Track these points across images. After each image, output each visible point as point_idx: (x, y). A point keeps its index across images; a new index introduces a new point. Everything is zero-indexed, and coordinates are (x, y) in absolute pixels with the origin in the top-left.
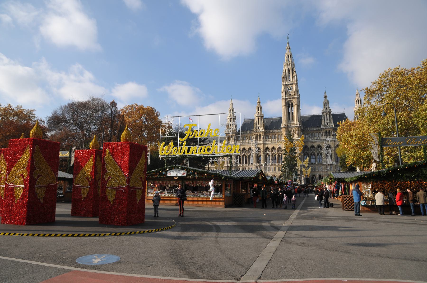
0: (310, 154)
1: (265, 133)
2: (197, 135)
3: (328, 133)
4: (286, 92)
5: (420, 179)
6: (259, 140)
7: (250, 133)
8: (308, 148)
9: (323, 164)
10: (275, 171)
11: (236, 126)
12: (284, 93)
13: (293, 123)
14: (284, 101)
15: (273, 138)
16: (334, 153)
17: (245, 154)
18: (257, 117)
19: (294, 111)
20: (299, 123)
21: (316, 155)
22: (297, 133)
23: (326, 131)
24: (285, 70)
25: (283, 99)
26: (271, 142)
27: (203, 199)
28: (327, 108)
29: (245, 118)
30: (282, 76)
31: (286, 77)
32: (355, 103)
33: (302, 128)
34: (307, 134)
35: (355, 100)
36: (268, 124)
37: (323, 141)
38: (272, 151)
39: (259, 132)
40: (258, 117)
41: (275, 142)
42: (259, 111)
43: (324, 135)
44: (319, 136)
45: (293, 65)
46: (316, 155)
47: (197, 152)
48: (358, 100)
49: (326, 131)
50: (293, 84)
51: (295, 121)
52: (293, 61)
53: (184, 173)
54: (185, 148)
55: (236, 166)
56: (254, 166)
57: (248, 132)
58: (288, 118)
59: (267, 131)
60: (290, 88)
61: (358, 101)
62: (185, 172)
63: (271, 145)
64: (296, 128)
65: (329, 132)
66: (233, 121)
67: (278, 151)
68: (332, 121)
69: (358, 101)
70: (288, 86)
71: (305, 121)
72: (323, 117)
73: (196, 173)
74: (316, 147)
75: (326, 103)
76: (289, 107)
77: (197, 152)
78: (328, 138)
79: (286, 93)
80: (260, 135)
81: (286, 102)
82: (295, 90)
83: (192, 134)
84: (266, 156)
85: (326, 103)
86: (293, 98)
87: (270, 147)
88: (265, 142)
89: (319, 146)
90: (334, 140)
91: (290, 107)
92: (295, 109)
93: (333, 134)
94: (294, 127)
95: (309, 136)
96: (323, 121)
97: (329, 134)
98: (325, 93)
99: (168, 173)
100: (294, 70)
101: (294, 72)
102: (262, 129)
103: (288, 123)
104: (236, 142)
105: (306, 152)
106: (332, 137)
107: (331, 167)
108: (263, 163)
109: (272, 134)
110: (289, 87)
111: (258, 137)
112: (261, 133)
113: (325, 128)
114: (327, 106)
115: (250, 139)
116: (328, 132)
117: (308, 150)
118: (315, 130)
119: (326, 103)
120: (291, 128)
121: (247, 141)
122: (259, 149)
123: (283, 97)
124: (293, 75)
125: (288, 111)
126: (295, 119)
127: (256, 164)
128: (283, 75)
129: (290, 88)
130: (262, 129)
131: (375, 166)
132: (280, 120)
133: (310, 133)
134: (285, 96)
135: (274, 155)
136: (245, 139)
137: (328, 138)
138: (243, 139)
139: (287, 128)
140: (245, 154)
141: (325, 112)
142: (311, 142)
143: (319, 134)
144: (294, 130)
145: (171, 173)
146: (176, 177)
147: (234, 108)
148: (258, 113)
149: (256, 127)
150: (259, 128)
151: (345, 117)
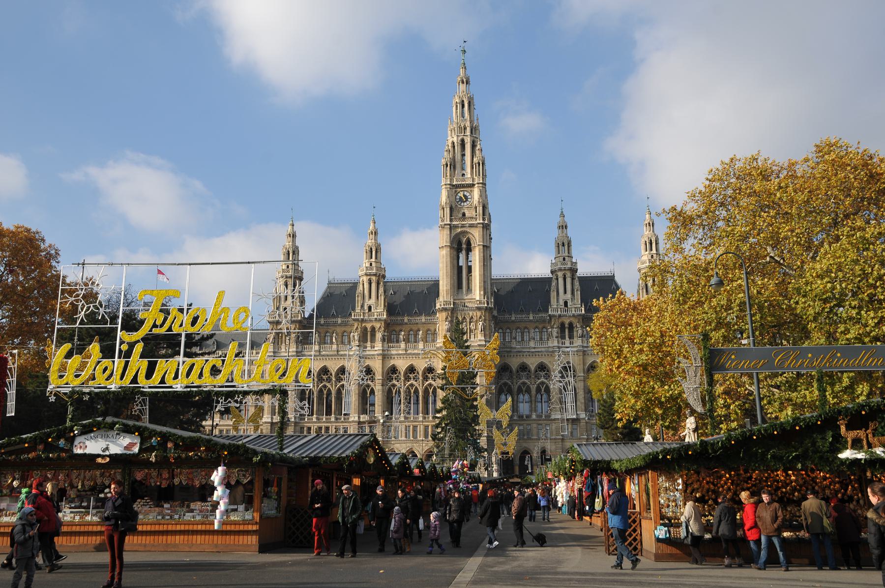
1: (388, 325)
2: (181, 325)
3: (567, 330)
4: (454, 206)
5: (811, 466)
6: (369, 343)
7: (345, 324)
8: (511, 372)
9: (552, 420)
10: (413, 437)
11: (302, 302)
12: (447, 211)
13: (469, 297)
14: (446, 232)
15: (412, 338)
16: (582, 387)
17: (328, 385)
18: (366, 275)
19: (475, 264)
20: (488, 298)
21: (534, 392)
22: (480, 327)
23: (563, 325)
24: (453, 143)
25: (442, 227)
26: (406, 350)
27: (191, 528)
28: (567, 258)
29: (331, 278)
30: (443, 162)
31: (452, 165)
32: (643, 247)
33: (495, 313)
34: (508, 331)
35: (643, 241)
36: (399, 299)
37: (553, 352)
38: (407, 378)
39: (371, 321)
40: (370, 275)
41: (416, 351)
42: (373, 259)
43: (555, 334)
44: (541, 339)
45: (474, 130)
46: (534, 392)
47: (176, 377)
48: (651, 241)
49: (563, 325)
50: (473, 185)
51: (477, 294)
52: (475, 118)
53: (131, 445)
54: (138, 364)
55: (297, 421)
56: (353, 421)
57: (339, 320)
58: (456, 281)
59: (393, 318)
60: (464, 195)
61: (651, 243)
62: (136, 441)
63: (404, 362)
64: (479, 314)
65: (571, 327)
66: (295, 286)
67: (426, 378)
68: (578, 294)
69: (651, 243)
70: (459, 190)
71: (502, 293)
72: (554, 284)
73: (170, 445)
74: (533, 368)
75: (564, 245)
76: (459, 250)
77: (176, 377)
78: (567, 344)
79: (451, 209)
80: (373, 329)
81: (453, 235)
82: (479, 202)
83: (165, 319)
84: (390, 391)
85: (563, 245)
86: (471, 226)
87: (402, 365)
88: (386, 353)
89: (542, 367)
90: (584, 351)
91: (464, 252)
92: (476, 257)
93: (580, 332)
94: (471, 309)
95: (515, 338)
96: (553, 294)
97: (569, 332)
98: (562, 215)
99: (76, 443)
100: (476, 146)
101: (477, 152)
102: (380, 311)
103: (455, 298)
104: (300, 350)
105: (505, 384)
106: (578, 342)
107: (575, 427)
108: (379, 415)
109: (407, 328)
110: (462, 193)
111: (366, 336)
112: (377, 325)
113: (560, 316)
114: (567, 251)
115: (344, 339)
116: (567, 326)
117: (511, 377)
118: (531, 321)
119: (563, 243)
120: (463, 313)
121: (334, 347)
122: (369, 371)
123: (443, 221)
124: (475, 159)
125: (455, 261)
126: (475, 286)
127: (359, 417)
128: (446, 158)
129: (464, 196)
130: (380, 314)
131: (694, 426)
132: (433, 288)
133: (516, 330)
134: (448, 220)
135: (412, 391)
136: (328, 339)
137: (567, 344)
138: (322, 342)
139: (453, 311)
140: (328, 385)
141: (560, 270)
142: (519, 354)
143: (541, 332)
144: (472, 317)
145: (87, 443)
146: (103, 457)
147: (297, 248)
148: (371, 264)
149: (362, 306)
150: (370, 308)
151: (614, 285)
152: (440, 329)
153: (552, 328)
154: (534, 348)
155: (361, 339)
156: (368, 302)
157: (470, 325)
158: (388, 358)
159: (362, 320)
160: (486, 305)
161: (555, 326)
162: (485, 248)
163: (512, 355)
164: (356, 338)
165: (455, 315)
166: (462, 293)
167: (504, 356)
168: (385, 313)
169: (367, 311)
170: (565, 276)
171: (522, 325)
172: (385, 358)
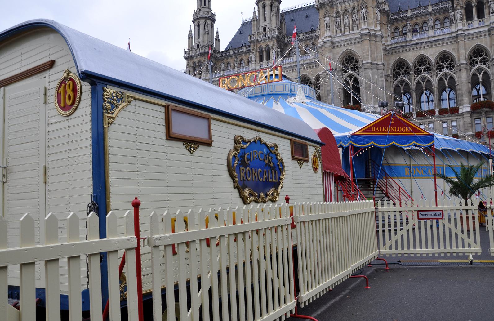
0: (413, 84)
6: (265, 61)
8: (407, 68)
37: (457, 37)
74: (433, 59)
89: (445, 57)
112: (271, 44)
118: (430, 13)
142: (415, 47)
144: (354, 8)
149: (258, 29)
154: (434, 37)
155: (258, 59)
156: (262, 24)
157: (352, 16)
159: (257, 40)
164: (253, 58)
165: (335, 10)
167: (399, 52)
168: (276, 31)
171: (420, 20)
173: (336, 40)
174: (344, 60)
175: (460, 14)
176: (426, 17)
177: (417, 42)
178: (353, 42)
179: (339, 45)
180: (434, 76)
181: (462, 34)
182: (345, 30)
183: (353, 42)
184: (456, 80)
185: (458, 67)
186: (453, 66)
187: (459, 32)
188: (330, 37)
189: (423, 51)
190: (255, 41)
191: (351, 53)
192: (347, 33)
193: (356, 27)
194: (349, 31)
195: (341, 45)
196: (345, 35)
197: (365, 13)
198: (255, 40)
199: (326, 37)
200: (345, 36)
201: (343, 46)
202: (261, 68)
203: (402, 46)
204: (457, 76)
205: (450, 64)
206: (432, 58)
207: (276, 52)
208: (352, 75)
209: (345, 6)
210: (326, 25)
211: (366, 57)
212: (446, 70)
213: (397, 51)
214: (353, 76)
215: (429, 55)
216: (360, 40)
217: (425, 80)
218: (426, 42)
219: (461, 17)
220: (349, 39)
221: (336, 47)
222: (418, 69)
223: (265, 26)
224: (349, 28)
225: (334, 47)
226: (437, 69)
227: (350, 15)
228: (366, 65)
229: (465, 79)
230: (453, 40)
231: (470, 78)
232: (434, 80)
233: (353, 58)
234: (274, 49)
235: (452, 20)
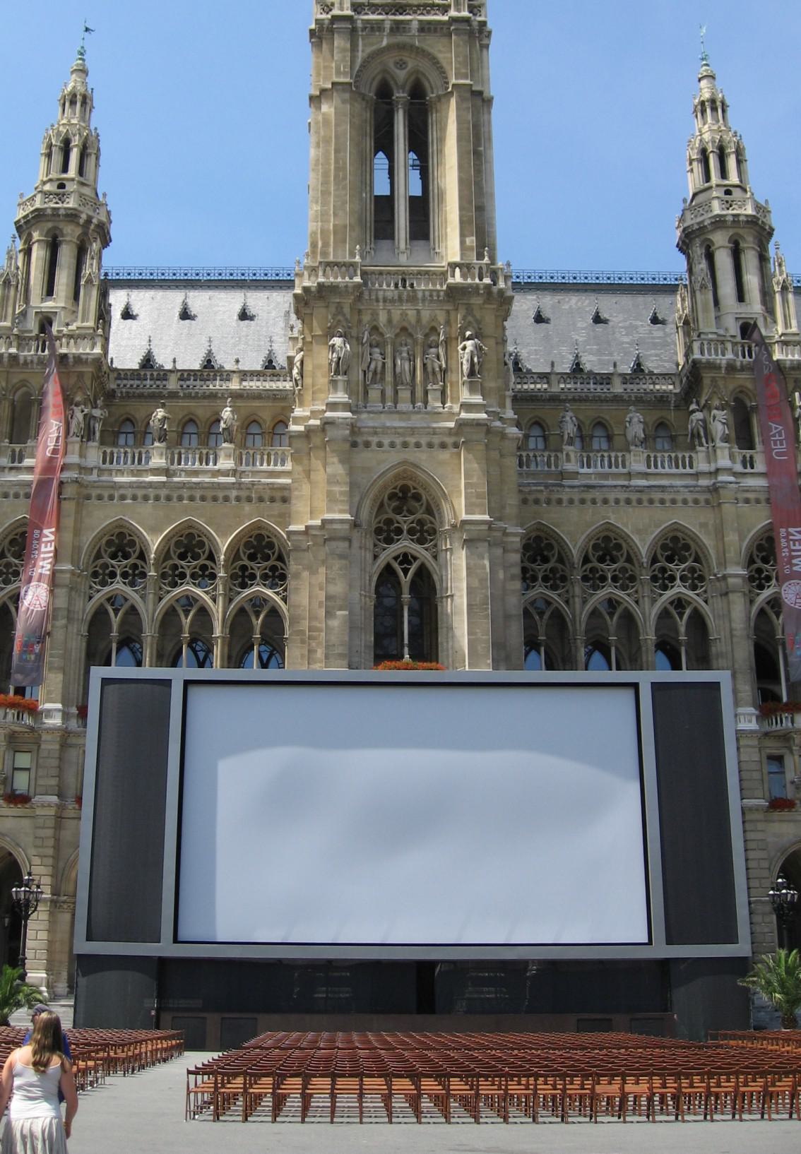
22: (467, 356)
28: (737, 193)
37: (715, 489)
43: (718, 429)
74: (643, 546)
81: (360, 56)
113: (731, 368)
141: (719, 222)
152: (308, 367)
153: (706, 407)
157: (424, 353)
158: (100, 498)
160: (487, 281)
161: (716, 402)
162: (479, 103)
163: (565, 497)
165: (366, 318)
166: (393, 249)
169: (36, 332)
170: (736, 244)
172: (88, 497)
173: (367, 420)
174: (386, 497)
175: (724, 423)
176: (605, 407)
177: (593, 482)
178: (423, 441)
179: (374, 440)
180: (646, 602)
181: (731, 483)
182: (396, 392)
183: (423, 441)
184: (712, 623)
185: (718, 584)
186: (701, 578)
187: (723, 478)
188: (347, 407)
189: (613, 513)
190: (6, 360)
191: (413, 478)
192: (404, 406)
193: (439, 394)
194: (413, 402)
195: (380, 445)
196: (398, 412)
197: (476, 352)
198: (6, 355)
199: (332, 406)
200: (396, 416)
201: (386, 447)
202: (16, 464)
203: (547, 486)
204: (713, 611)
205: (692, 570)
206: (640, 540)
207: (85, 416)
208: (412, 556)
209: (401, 314)
210: (338, 363)
211: (474, 500)
212: (679, 589)
213: (531, 498)
214: (415, 558)
215: (630, 527)
216: (450, 440)
217: (615, 608)
218: (623, 486)
219: (727, 432)
220: (412, 428)
221: (361, 446)
222: (663, 570)
223: (50, 315)
224: (413, 393)
225: (354, 444)
226: (654, 579)
227: (419, 350)
228: (473, 527)
229: (742, 626)
230: (702, 497)
231: (752, 624)
232: (644, 614)
233: (417, 497)
234: (77, 405)
235: (699, 434)
